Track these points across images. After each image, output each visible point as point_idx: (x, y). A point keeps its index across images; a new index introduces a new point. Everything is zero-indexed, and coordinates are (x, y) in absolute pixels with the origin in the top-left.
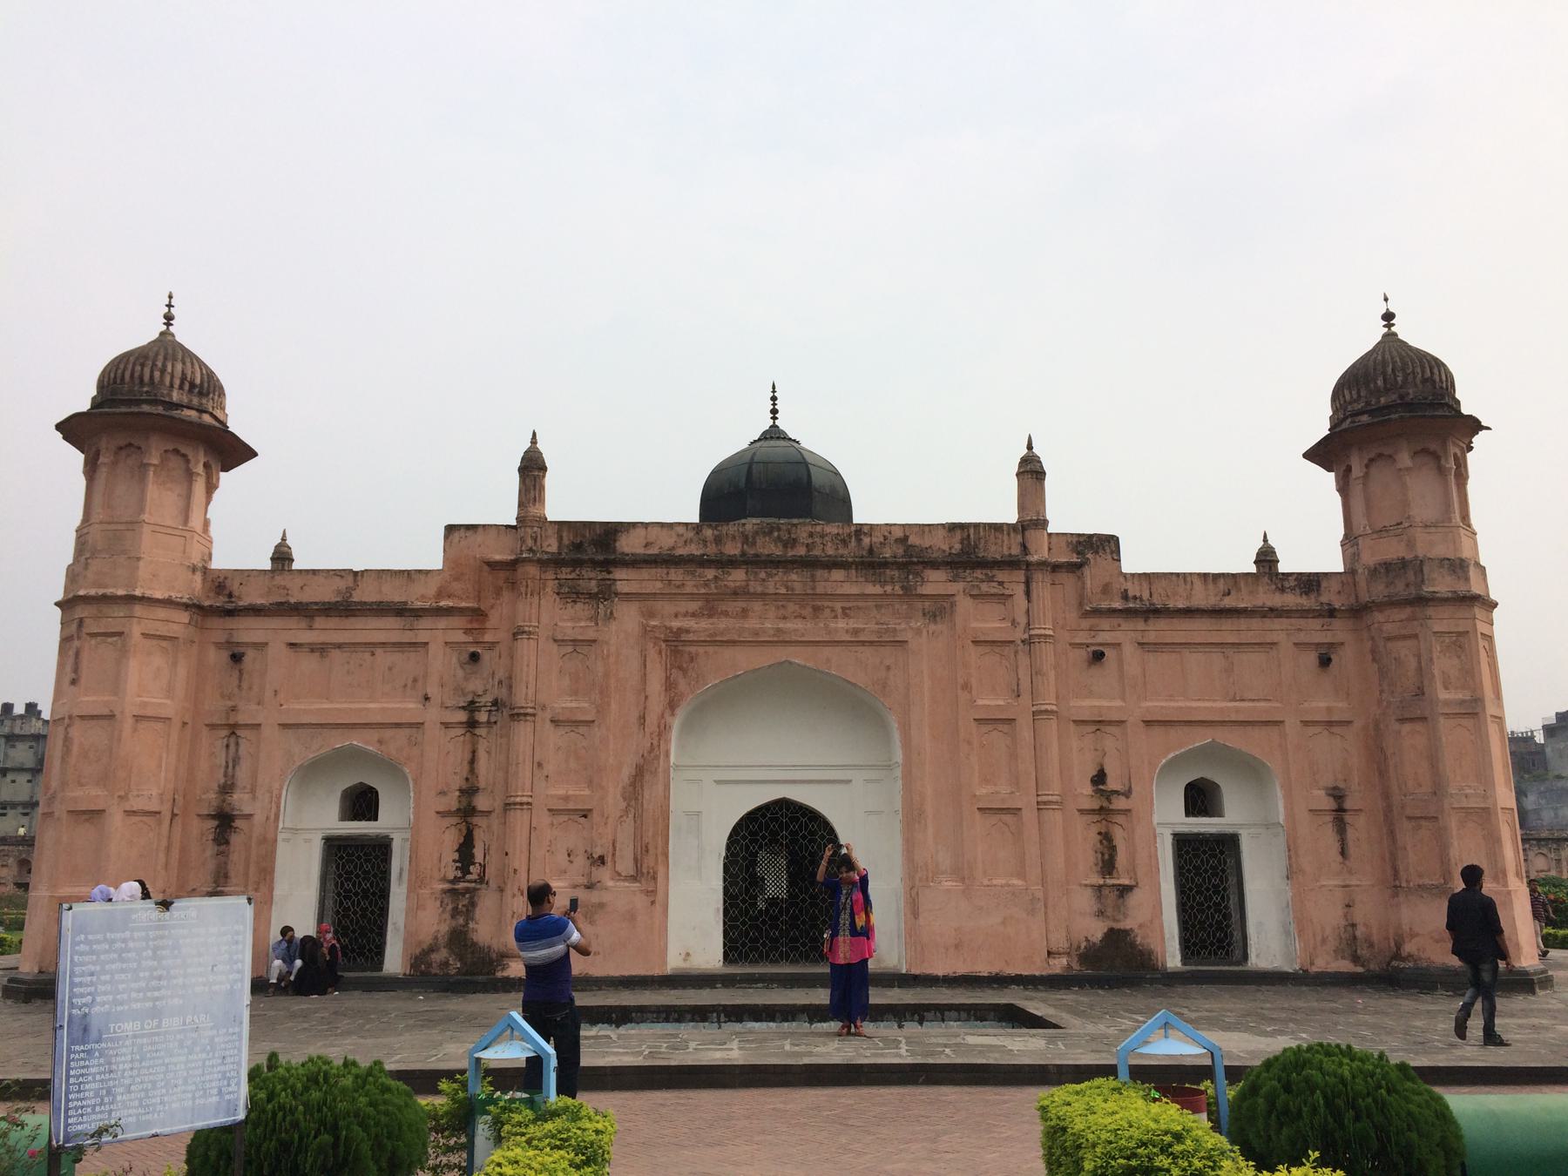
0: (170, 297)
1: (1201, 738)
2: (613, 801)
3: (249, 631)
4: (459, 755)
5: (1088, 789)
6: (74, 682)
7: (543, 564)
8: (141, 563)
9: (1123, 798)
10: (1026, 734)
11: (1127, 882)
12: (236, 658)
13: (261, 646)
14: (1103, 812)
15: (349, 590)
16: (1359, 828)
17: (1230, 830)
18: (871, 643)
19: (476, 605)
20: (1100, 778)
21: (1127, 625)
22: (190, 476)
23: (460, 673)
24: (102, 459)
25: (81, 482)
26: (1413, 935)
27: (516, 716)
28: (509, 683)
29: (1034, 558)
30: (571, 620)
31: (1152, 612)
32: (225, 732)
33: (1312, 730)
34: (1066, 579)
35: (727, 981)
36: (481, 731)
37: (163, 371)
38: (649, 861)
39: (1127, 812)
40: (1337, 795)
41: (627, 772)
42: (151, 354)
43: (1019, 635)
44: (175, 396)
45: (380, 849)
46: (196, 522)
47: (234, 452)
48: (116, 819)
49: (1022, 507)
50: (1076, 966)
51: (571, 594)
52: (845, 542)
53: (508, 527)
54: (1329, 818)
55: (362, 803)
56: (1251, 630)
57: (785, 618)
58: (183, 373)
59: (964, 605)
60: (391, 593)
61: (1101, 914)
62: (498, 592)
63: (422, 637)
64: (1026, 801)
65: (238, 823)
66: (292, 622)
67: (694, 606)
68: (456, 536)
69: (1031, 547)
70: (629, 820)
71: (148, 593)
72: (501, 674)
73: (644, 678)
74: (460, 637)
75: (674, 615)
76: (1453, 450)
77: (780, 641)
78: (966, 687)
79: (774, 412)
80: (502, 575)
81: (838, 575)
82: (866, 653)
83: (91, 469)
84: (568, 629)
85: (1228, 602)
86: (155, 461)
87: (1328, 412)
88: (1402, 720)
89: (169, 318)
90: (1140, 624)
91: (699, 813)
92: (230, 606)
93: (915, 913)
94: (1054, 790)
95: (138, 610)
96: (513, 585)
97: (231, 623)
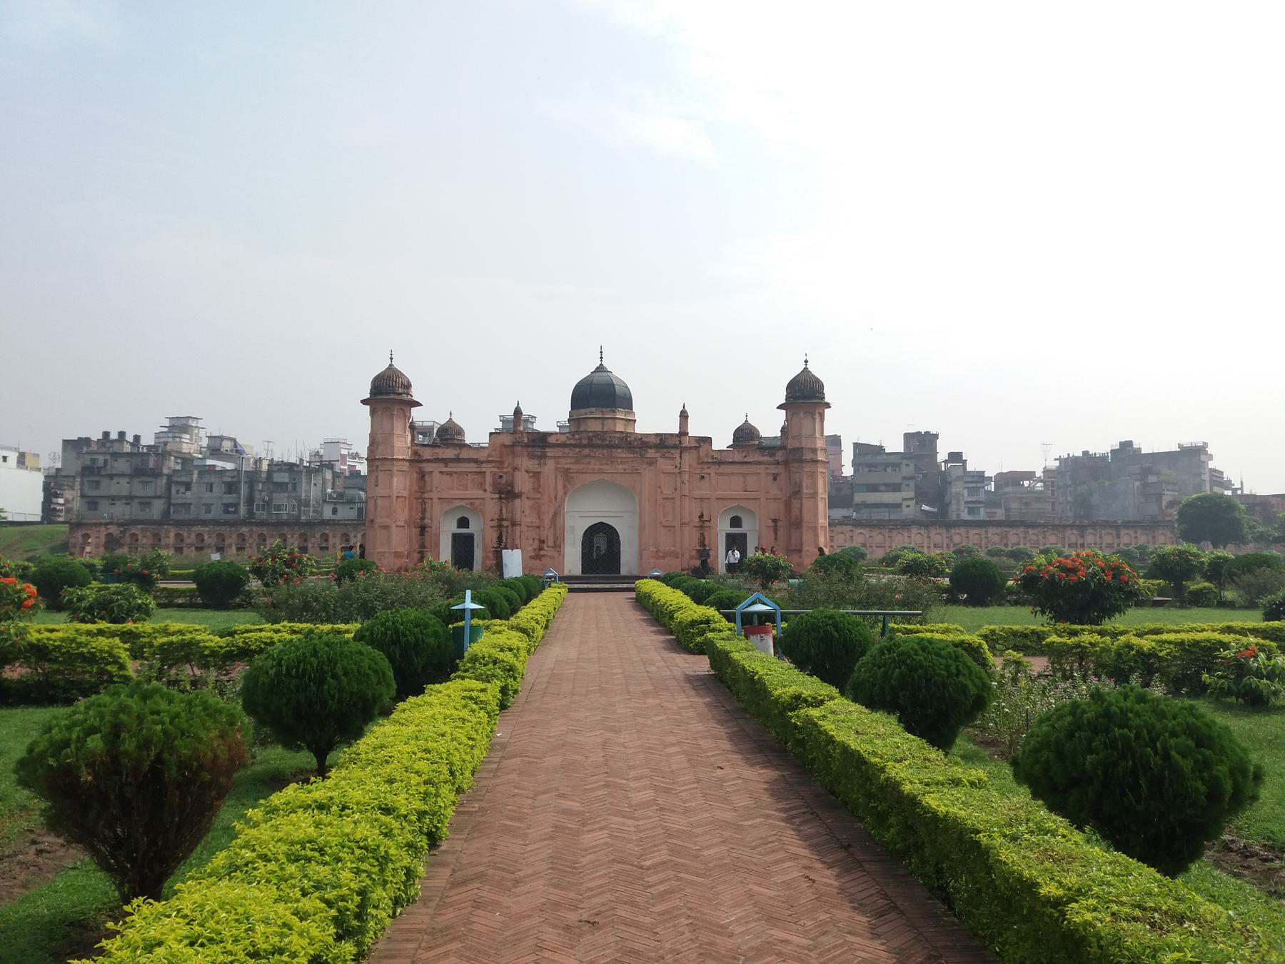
1: (734, 504)
2: (547, 522)
3: (428, 467)
4: (496, 509)
16: (781, 533)
20: (701, 516)
28: (512, 485)
30: (531, 464)
31: (720, 463)
34: (694, 452)
40: (775, 521)
45: (470, 538)
48: (394, 529)
51: (532, 456)
55: (463, 522)
56: (753, 469)
59: (660, 461)
66: (441, 465)
75: (565, 464)
77: (601, 472)
83: (373, 413)
84: (531, 468)
94: (686, 520)
96: (513, 453)
97: (421, 465)
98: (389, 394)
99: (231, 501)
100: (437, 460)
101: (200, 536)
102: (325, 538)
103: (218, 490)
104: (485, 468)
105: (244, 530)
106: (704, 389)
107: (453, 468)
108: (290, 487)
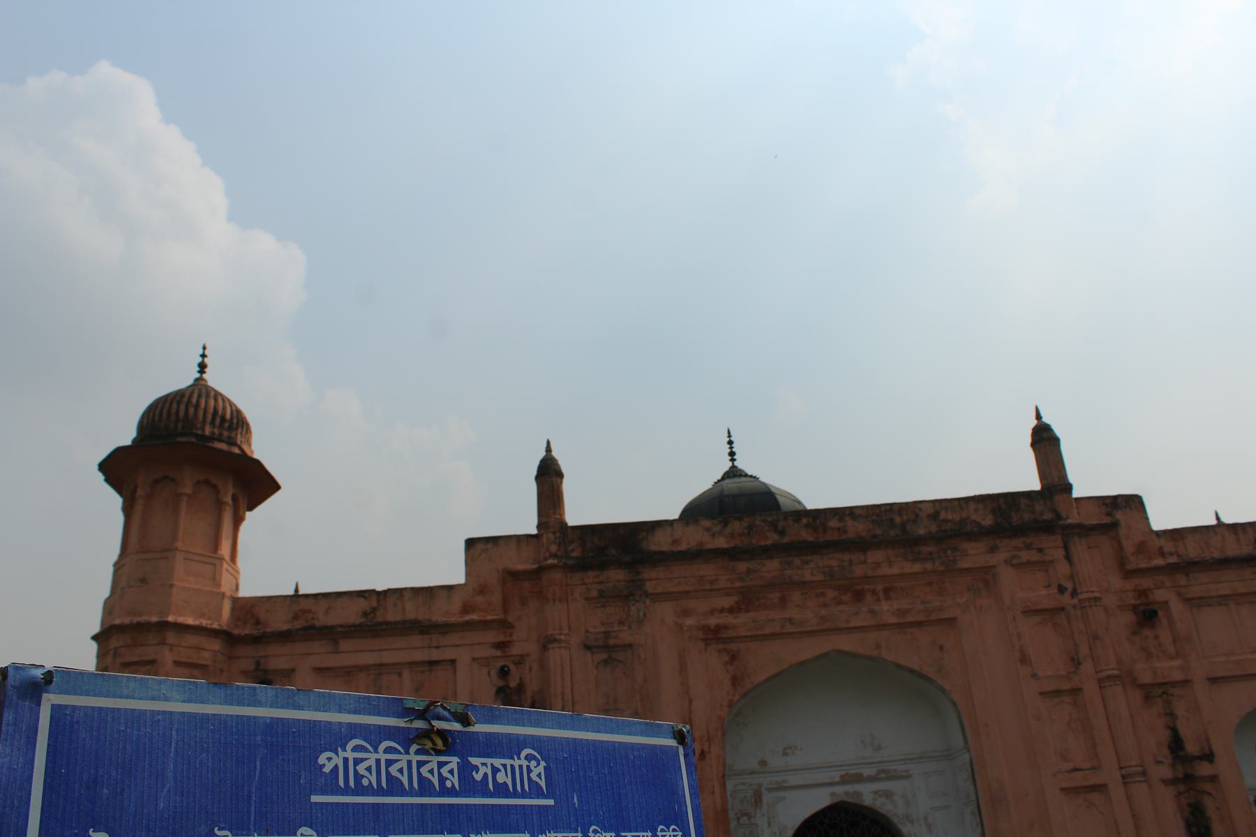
0: (204, 348)
8: (175, 590)
9: (1205, 763)
15: (374, 610)
18: (919, 624)
19: (502, 617)
20: (1176, 744)
22: (220, 505)
24: (140, 492)
25: (120, 519)
31: (1189, 566)
37: (197, 406)
42: (187, 396)
44: (207, 433)
46: (225, 550)
47: (257, 484)
49: (1043, 475)
57: (825, 605)
58: (215, 410)
60: (411, 611)
63: (448, 654)
66: (317, 647)
68: (480, 546)
71: (181, 620)
78: (1024, 659)
79: (732, 454)
81: (876, 556)
86: (188, 490)
89: (202, 367)
90: (1183, 581)
92: (255, 632)
95: (171, 637)
107: (355, 653)
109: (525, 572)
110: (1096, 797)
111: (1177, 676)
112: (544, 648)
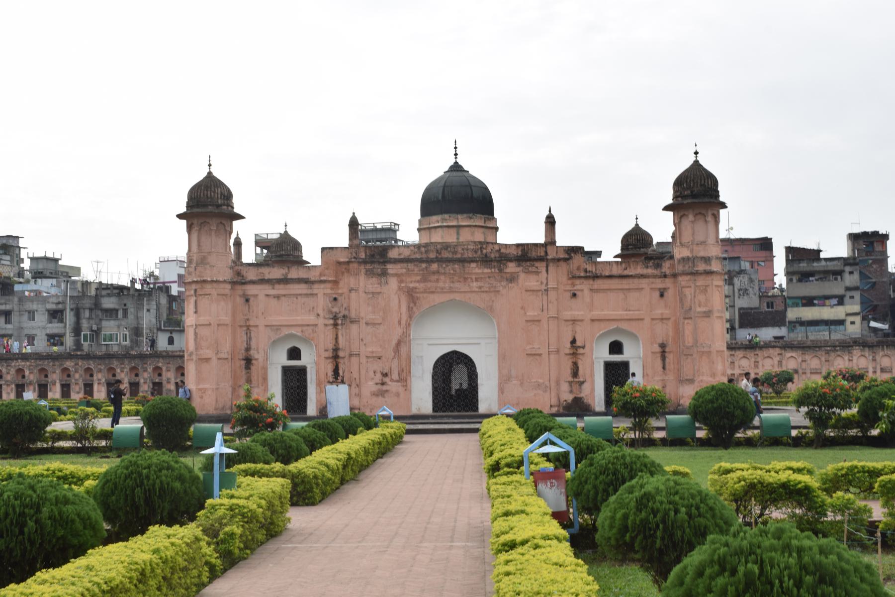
1: (613, 326)
3: (251, 290)
5: (569, 345)
6: (196, 312)
7: (360, 263)
10: (546, 326)
11: (582, 380)
12: (247, 300)
13: (256, 296)
14: (574, 354)
15: (287, 274)
16: (670, 358)
17: (625, 360)
20: (574, 341)
21: (585, 282)
22: (226, 230)
23: (330, 305)
26: (683, 397)
27: (352, 322)
28: (348, 309)
29: (550, 257)
30: (372, 284)
32: (245, 329)
33: (655, 322)
35: (433, 417)
36: (340, 327)
37: (214, 192)
38: (404, 374)
39: (583, 354)
40: (663, 346)
41: (394, 342)
43: (544, 287)
44: (220, 202)
50: (561, 411)
51: (370, 273)
52: (476, 252)
53: (346, 248)
54: (659, 355)
55: (294, 353)
59: (522, 276)
61: (571, 392)
62: (343, 273)
63: (315, 291)
64: (544, 351)
65: (253, 362)
67: (418, 278)
68: (325, 251)
69: (549, 252)
70: (396, 360)
72: (345, 305)
73: (400, 306)
74: (329, 291)
76: (710, 213)
77: (451, 291)
79: (456, 154)
80: (344, 267)
81: (473, 265)
82: (484, 295)
83: (190, 228)
84: (370, 288)
85: (626, 273)
87: (672, 192)
88: (685, 318)
90: (591, 282)
91: (422, 357)
93: (502, 393)
95: (215, 285)
98: (209, 205)
99: (55, 331)
100: (263, 281)
101: (20, 371)
102: (158, 371)
103: (41, 319)
104: (318, 289)
105: (69, 364)
106: (577, 188)
107: (280, 290)
108: (120, 313)
109: (344, 263)
110: (538, 357)
111: (580, 318)
112: (350, 291)
